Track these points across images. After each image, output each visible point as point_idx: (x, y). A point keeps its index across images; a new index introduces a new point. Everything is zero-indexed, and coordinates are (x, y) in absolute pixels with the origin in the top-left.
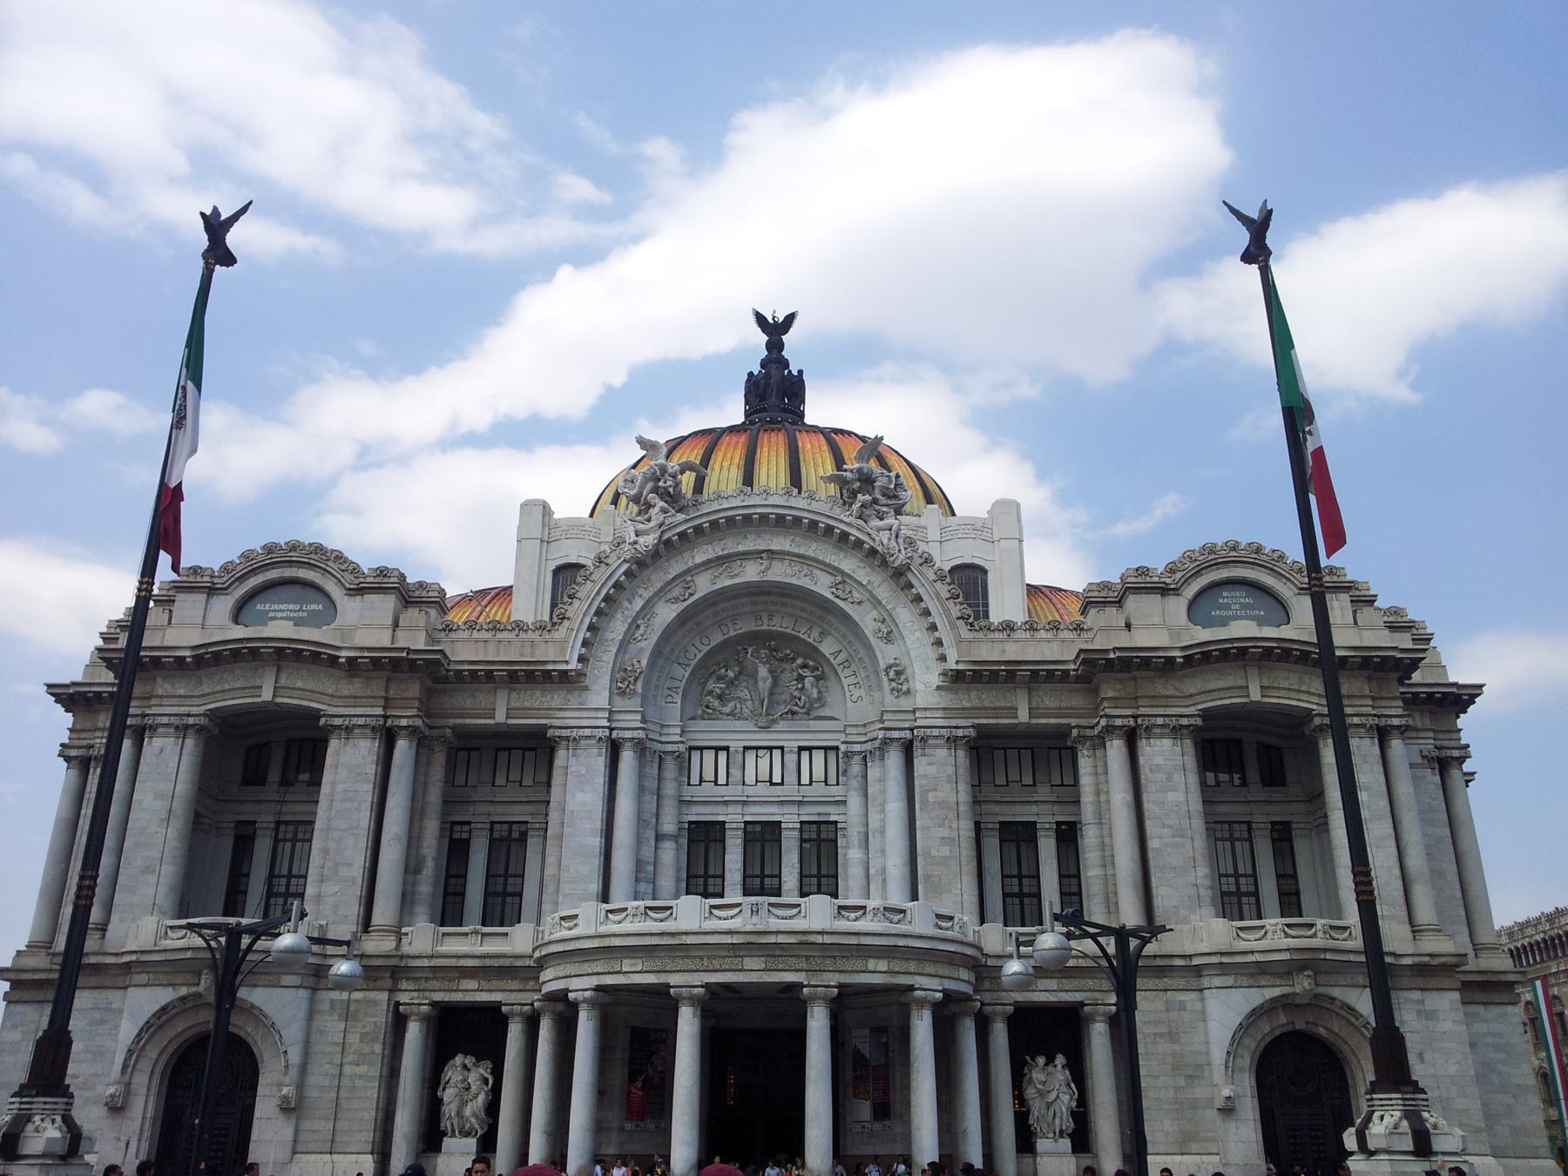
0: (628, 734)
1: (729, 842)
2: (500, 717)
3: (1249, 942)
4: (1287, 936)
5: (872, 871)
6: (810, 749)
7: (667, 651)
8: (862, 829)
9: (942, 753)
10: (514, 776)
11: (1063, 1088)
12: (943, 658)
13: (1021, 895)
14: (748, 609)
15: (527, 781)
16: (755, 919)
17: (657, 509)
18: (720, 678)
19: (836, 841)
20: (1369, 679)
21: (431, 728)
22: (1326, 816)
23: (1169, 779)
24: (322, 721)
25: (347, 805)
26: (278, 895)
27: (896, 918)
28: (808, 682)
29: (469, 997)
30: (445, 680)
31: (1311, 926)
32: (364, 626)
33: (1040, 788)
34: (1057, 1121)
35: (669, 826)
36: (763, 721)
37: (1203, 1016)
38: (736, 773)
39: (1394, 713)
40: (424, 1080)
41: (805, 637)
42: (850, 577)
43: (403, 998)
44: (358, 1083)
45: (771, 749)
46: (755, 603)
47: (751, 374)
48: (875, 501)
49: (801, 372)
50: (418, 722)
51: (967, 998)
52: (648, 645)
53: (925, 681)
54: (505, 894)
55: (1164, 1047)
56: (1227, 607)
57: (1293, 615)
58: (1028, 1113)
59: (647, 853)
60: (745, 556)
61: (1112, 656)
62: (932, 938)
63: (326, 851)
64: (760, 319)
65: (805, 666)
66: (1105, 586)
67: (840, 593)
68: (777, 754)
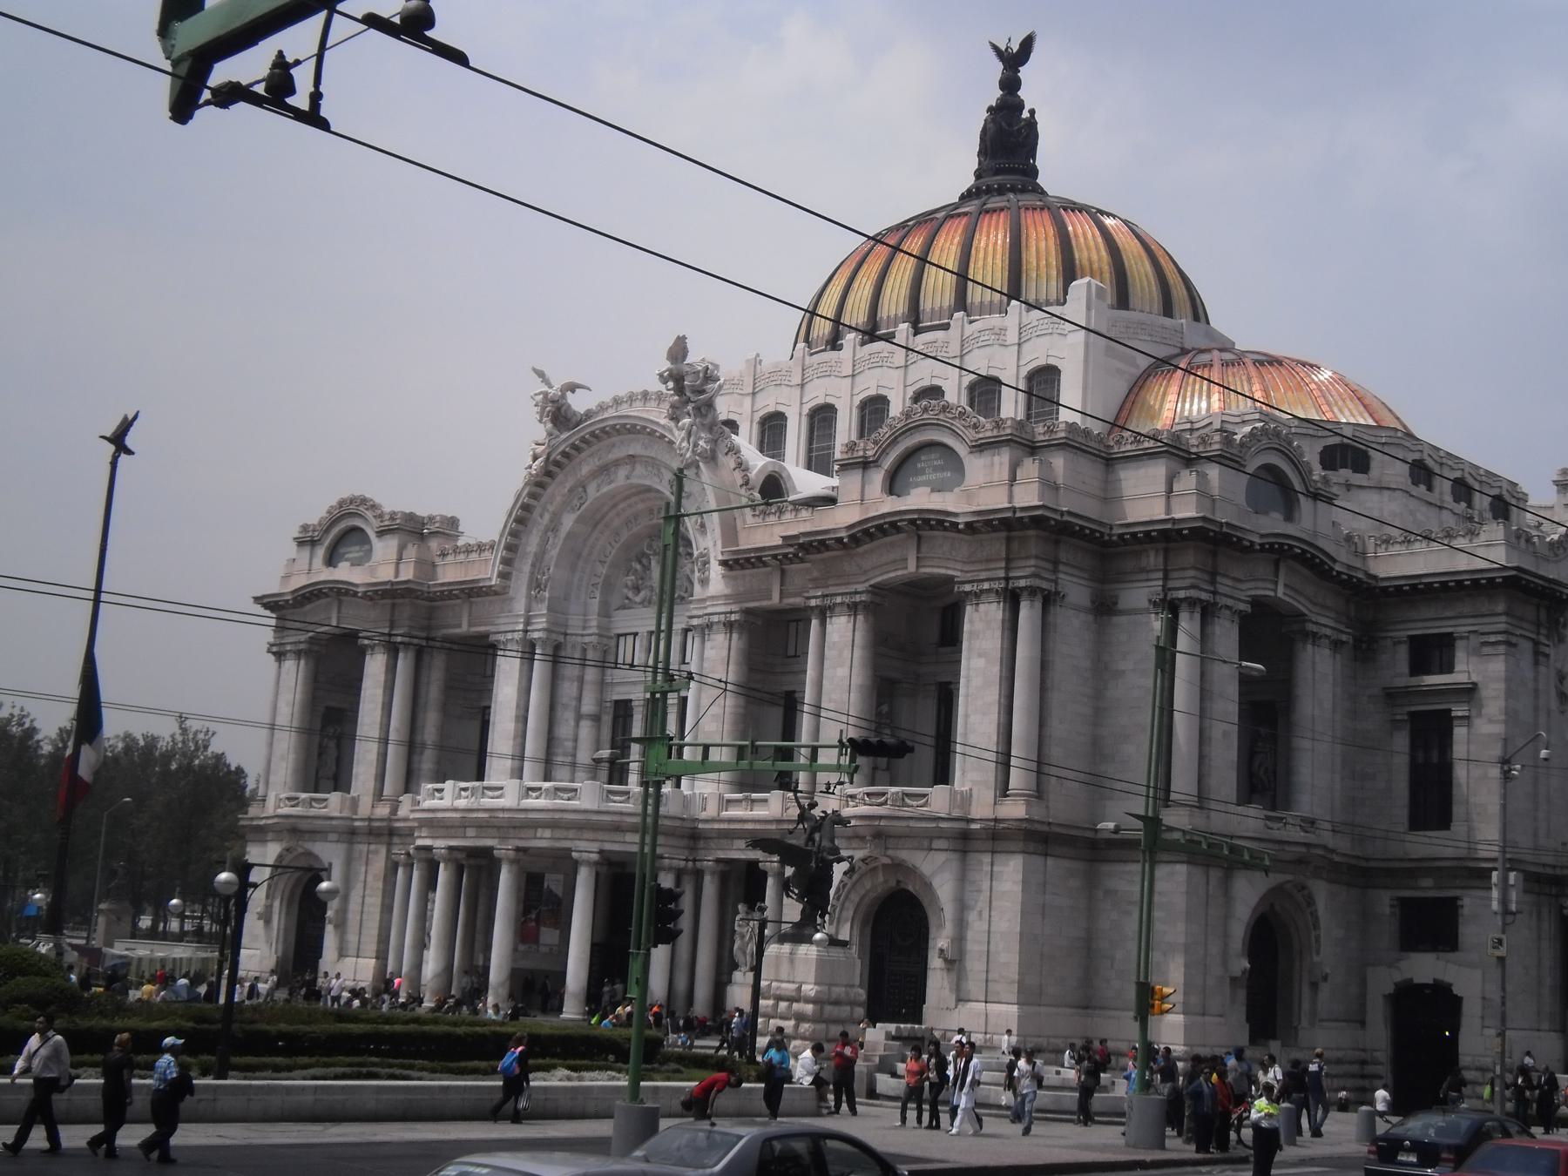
0: (536, 635)
7: (585, 553)
21: (427, 639)
31: (884, 794)
32: (383, 563)
35: (588, 706)
46: (643, 501)
49: (1032, 112)
52: (554, 553)
53: (716, 571)
56: (922, 472)
60: (617, 463)
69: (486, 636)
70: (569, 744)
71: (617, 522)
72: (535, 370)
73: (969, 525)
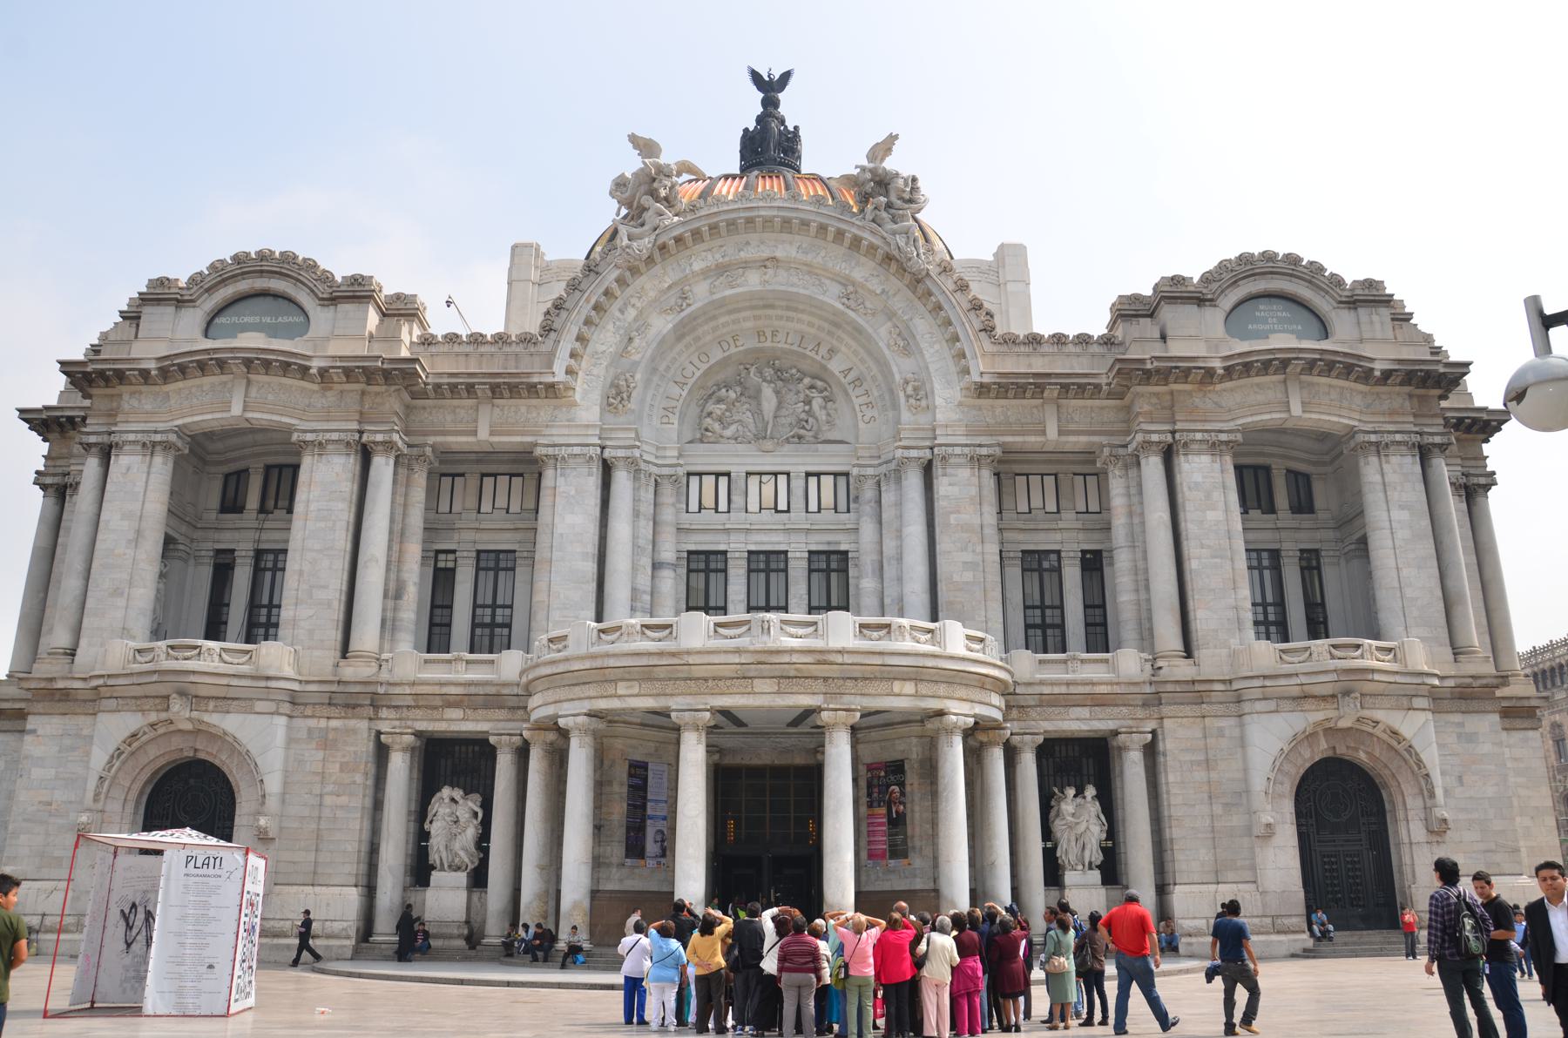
0: (621, 453)
1: (731, 572)
2: (483, 434)
3: (1295, 664)
4: (1333, 657)
5: (887, 601)
6: (818, 475)
7: (662, 368)
8: (875, 557)
9: (965, 473)
10: (501, 502)
11: (1094, 820)
12: (966, 371)
13: (1043, 626)
14: (749, 324)
15: (515, 508)
16: (765, 638)
17: (650, 213)
18: (720, 401)
19: (846, 571)
20: (1410, 396)
22: (1363, 542)
23: (1208, 496)
24: (295, 437)
25: (322, 525)
26: (260, 625)
27: (923, 637)
28: (817, 403)
29: (455, 727)
30: (423, 395)
31: (1358, 646)
33: (1064, 515)
34: (1087, 854)
35: (668, 554)
36: (768, 445)
37: (1242, 742)
38: (738, 499)
39: (1435, 433)
40: (409, 813)
41: (812, 354)
42: (863, 286)
43: (384, 727)
44: (339, 814)
45: (776, 474)
46: (756, 318)
47: (746, 130)
48: (889, 206)
50: (396, 437)
51: (996, 726)
54: (493, 625)
55: (1200, 775)
56: (1264, 321)
58: (1055, 848)
59: (644, 581)
60: (746, 265)
61: (1149, 366)
62: (963, 659)
63: (301, 573)
64: (756, 77)
65: (812, 387)
66: (1136, 298)
67: (852, 303)
68: (782, 479)
70: (647, 598)
71: (709, 338)
72: (634, 140)
73: (1387, 375)
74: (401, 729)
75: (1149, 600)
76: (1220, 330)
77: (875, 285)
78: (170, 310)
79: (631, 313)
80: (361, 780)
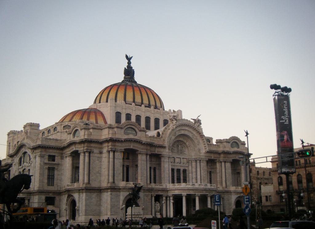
5: (193, 177)
8: (191, 171)
28: (184, 148)
29: (160, 194)
43: (152, 194)
47: (125, 68)
49: (134, 70)
53: (203, 151)
57: (240, 147)
64: (127, 57)
69: (161, 154)
74: (154, 194)
75: (222, 180)
76: (230, 146)
77: (196, 135)
78: (120, 129)
79: (171, 136)
80: (151, 201)
